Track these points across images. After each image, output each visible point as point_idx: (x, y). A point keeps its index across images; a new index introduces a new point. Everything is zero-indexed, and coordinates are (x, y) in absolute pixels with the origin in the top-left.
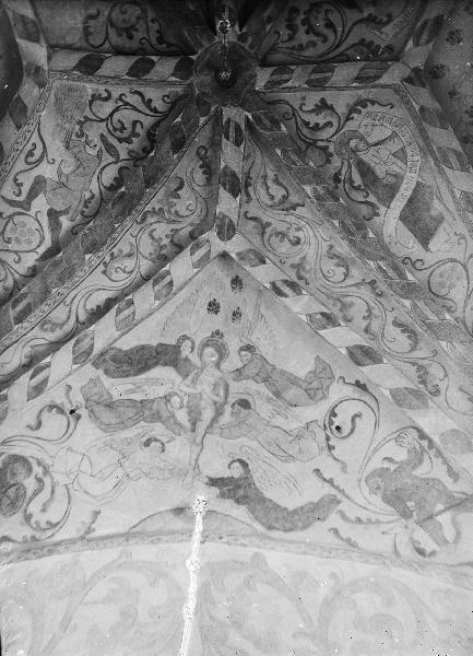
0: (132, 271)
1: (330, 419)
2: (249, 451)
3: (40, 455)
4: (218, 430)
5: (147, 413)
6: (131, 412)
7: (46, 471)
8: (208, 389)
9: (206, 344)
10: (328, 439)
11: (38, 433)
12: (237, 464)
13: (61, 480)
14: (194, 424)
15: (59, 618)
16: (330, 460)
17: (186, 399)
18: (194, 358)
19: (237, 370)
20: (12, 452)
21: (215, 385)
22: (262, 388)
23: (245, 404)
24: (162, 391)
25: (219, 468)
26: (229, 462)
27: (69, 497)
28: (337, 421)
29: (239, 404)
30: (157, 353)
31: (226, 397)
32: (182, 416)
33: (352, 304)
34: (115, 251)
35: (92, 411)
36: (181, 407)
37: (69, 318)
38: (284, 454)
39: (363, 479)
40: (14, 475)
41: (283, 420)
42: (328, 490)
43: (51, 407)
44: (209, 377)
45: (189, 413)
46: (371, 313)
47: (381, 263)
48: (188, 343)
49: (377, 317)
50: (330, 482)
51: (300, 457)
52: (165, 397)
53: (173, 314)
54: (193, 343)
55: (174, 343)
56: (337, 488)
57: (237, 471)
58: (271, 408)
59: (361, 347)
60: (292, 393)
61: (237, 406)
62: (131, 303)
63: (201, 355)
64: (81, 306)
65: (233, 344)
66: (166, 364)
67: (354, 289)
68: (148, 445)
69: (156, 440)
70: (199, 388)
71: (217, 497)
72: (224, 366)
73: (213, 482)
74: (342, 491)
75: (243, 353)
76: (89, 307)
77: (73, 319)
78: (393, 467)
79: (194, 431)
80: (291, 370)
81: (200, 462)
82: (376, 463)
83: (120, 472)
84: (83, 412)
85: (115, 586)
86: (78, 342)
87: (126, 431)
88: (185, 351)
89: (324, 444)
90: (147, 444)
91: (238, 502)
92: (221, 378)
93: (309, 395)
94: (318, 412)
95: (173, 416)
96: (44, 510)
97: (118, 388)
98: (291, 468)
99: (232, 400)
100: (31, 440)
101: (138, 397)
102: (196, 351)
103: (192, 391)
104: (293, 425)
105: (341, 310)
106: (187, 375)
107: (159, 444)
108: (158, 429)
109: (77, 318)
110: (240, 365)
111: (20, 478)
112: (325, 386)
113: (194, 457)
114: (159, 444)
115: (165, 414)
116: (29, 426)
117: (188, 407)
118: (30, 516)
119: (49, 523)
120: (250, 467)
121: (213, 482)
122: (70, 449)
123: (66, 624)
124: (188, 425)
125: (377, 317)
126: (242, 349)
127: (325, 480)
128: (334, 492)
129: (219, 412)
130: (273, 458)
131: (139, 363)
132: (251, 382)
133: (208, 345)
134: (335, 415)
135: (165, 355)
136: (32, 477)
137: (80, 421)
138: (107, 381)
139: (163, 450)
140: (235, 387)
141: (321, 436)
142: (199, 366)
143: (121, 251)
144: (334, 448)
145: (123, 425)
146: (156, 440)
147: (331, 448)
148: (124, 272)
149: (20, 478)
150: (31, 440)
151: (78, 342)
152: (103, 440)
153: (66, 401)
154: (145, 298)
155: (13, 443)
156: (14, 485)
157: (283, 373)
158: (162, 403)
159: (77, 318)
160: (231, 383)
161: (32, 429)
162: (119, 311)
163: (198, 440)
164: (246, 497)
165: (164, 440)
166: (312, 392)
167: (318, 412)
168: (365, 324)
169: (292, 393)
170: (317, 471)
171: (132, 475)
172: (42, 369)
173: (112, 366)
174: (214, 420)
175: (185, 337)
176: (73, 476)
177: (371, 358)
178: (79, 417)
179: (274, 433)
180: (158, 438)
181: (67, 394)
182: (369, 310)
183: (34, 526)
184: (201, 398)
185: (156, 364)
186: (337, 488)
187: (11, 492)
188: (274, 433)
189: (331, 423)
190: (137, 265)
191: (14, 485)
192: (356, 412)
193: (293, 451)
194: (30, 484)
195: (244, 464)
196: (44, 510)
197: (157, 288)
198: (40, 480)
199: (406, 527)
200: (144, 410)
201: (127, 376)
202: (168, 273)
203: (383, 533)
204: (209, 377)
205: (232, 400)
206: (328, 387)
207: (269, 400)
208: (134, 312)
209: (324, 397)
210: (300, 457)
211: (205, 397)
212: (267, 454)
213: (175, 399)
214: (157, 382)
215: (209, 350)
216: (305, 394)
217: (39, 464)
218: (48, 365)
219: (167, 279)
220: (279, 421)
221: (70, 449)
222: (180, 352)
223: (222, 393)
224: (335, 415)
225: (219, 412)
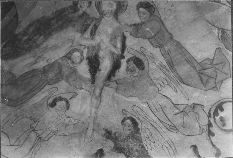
2: (140, 112)
4: (114, 85)
10: (210, 125)
12: (129, 121)
16: (208, 144)
17: (85, 51)
19: (135, 25)
21: (113, 39)
24: (61, 53)
25: (114, 121)
29: (134, 62)
32: (83, 69)
36: (81, 60)
41: (174, 94)
44: (108, 27)
51: (181, 129)
52: (66, 56)
60: (184, 69)
61: (132, 65)
69: (61, 99)
70: (98, 39)
71: (112, 150)
72: (123, 16)
75: (141, 9)
79: (93, 81)
80: (188, 47)
89: (205, 128)
90: (53, 104)
92: (118, 29)
93: (201, 79)
95: (74, 71)
104: (181, 100)
107: (64, 102)
114: (64, 102)
117: (88, 58)
120: (140, 126)
124: (88, 76)
126: (141, 5)
129: (116, 66)
132: (146, 43)
134: (222, 110)
139: (68, 108)
141: (205, 121)
142: (98, 16)
144: (213, 135)
146: (61, 99)
147: (211, 134)
160: (127, 34)
163: (97, 92)
165: (67, 96)
166: (205, 78)
169: (184, 69)
170: (195, 148)
171: (44, 136)
179: (163, 102)
180: (64, 96)
188: (163, 102)
189: (216, 113)
193: (178, 121)
205: (128, 55)
206: (222, 81)
207: (161, 67)
210: (181, 129)
211: (103, 47)
212: (155, 119)
223: (119, 45)
224: (222, 110)
225: (116, 66)
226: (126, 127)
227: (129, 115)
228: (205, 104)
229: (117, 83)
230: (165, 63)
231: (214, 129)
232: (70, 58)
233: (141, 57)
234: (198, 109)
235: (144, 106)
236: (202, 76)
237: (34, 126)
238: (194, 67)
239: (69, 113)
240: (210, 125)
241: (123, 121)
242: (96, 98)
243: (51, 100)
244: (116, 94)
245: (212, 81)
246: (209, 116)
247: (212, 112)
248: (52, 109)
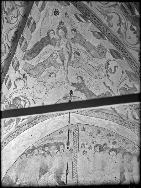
0: (17, 17)
1: (107, 65)
3: (21, 95)
4: (71, 64)
5: (47, 65)
6: (41, 67)
7: (25, 97)
8: (65, 47)
9: (58, 29)
10: (107, 72)
11: (16, 90)
12: (79, 78)
13: (30, 98)
14: (63, 62)
17: (58, 53)
18: (56, 37)
19: (73, 39)
20: (13, 98)
22: (82, 47)
23: (78, 54)
25: (74, 80)
26: (76, 77)
27: (34, 102)
28: (109, 67)
30: (42, 43)
31: (71, 50)
32: (59, 60)
33: (112, 16)
34: (6, 10)
35: (29, 73)
37: (6, 47)
38: (94, 75)
39: (119, 89)
40: (17, 103)
42: (108, 90)
43: (17, 80)
44: (63, 42)
45: (60, 58)
46: (121, 21)
47: (123, 4)
48: (52, 32)
49: (123, 24)
50: (109, 87)
53: (41, 25)
54: (53, 31)
55: (46, 35)
56: (111, 90)
57: (79, 81)
58: (87, 56)
59: (115, 51)
60: (93, 52)
62: (23, 38)
63: (58, 34)
64: (7, 41)
65: (69, 29)
66: (47, 45)
67: (113, 8)
68: (51, 76)
69: (53, 73)
72: (67, 36)
73: (73, 85)
74: (112, 91)
75: (73, 32)
76: (10, 40)
77: (7, 47)
78: (128, 89)
79: (63, 65)
81: (68, 77)
82: (122, 85)
83: (45, 88)
84: (27, 75)
86: (13, 64)
88: (52, 36)
89: (106, 74)
90: (50, 76)
91: (82, 92)
94: (103, 61)
95: (56, 62)
97: (34, 62)
98: (96, 80)
99: (73, 52)
101: (42, 61)
102: (55, 33)
103: (60, 49)
105: (107, 21)
106: (56, 44)
108: (52, 68)
109: (8, 46)
110: (73, 37)
112: (105, 52)
113: (66, 76)
115: (52, 62)
116: (13, 89)
121: (73, 85)
122: (28, 88)
124: (61, 63)
125: (123, 24)
127: (107, 86)
128: (110, 91)
129: (70, 57)
130: (90, 76)
131: (37, 50)
133: (59, 29)
134: (109, 65)
135: (46, 41)
136: (22, 101)
137: (27, 79)
138: (29, 62)
139: (56, 76)
140: (73, 45)
141: (105, 71)
143: (8, 9)
145: (41, 73)
146: (53, 73)
147: (108, 76)
148: (15, 17)
149: (19, 103)
150: (17, 92)
151: (13, 64)
152: (37, 80)
153: (20, 75)
154: (26, 34)
155: (12, 95)
157: (89, 43)
158: (51, 59)
159: (8, 46)
160: (71, 43)
161: (15, 89)
162: (21, 44)
163: (66, 69)
164: (84, 90)
165: (55, 72)
166: (100, 53)
167: (103, 61)
168: (118, 27)
169: (93, 52)
170: (104, 83)
171: (49, 88)
172: (7, 79)
173: (29, 57)
174: (69, 59)
175: (50, 31)
176: (33, 95)
177: (119, 56)
178: (26, 77)
179: (89, 67)
181: (19, 73)
182: (120, 20)
184: (63, 51)
185: (43, 47)
186: (111, 90)
190: (18, 12)
191: (18, 106)
192: (116, 65)
195: (82, 78)
197: (30, 27)
198: (24, 101)
199: (131, 109)
200: (45, 64)
201: (35, 56)
202: (31, 18)
203: (124, 109)
204: (63, 42)
206: (106, 53)
207: (86, 53)
208: (26, 42)
209: (105, 57)
210: (98, 76)
211: (64, 50)
212: (88, 74)
213: (55, 55)
214: (46, 52)
215: (61, 31)
216: (98, 53)
217: (22, 97)
218: (8, 76)
219: (32, 21)
220: (90, 62)
221: (28, 88)
222: (50, 37)
223: (69, 48)
224: (109, 65)
225: (70, 57)
226: (79, 81)
227: (79, 75)
228: (103, 64)
229: (72, 64)
230: (86, 51)
231: (109, 74)
232: (52, 57)
233: (78, 51)
234: (101, 66)
235: (83, 70)
236: (99, 53)
238: (96, 50)
239: (56, 78)
240: (107, 72)
241: (77, 78)
242: (66, 71)
243: (49, 74)
244: (73, 68)
245: (103, 54)
246: (106, 68)
247: (106, 67)
248: (50, 78)
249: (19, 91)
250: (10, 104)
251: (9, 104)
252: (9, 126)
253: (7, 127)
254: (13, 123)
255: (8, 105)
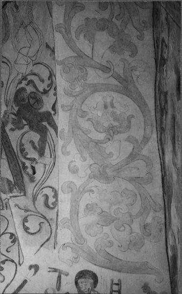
3: (17, 82)
13: (30, 67)
15: (100, 72)
20: (12, 100)
40: (23, 100)
83: (29, 28)
85: (82, 37)
87: (10, 22)
96: (42, 81)
100: (8, 87)
111: (26, 96)
118: (44, 90)
119: (49, 79)
122: (15, 62)
123: (105, 69)
149: (26, 96)
150: (8, 87)
156: (29, 100)
183: (49, 88)
187: (32, 101)
191: (29, 100)
194: (30, 89)
196: (42, 81)
217: (20, 83)
237: (25, 26)
243: (15, 9)
248: (19, 8)
249: (10, 82)
250: (15, 112)
251: (14, 114)
252: (47, 144)
253: (47, 151)
254: (48, 133)
255: (13, 117)
